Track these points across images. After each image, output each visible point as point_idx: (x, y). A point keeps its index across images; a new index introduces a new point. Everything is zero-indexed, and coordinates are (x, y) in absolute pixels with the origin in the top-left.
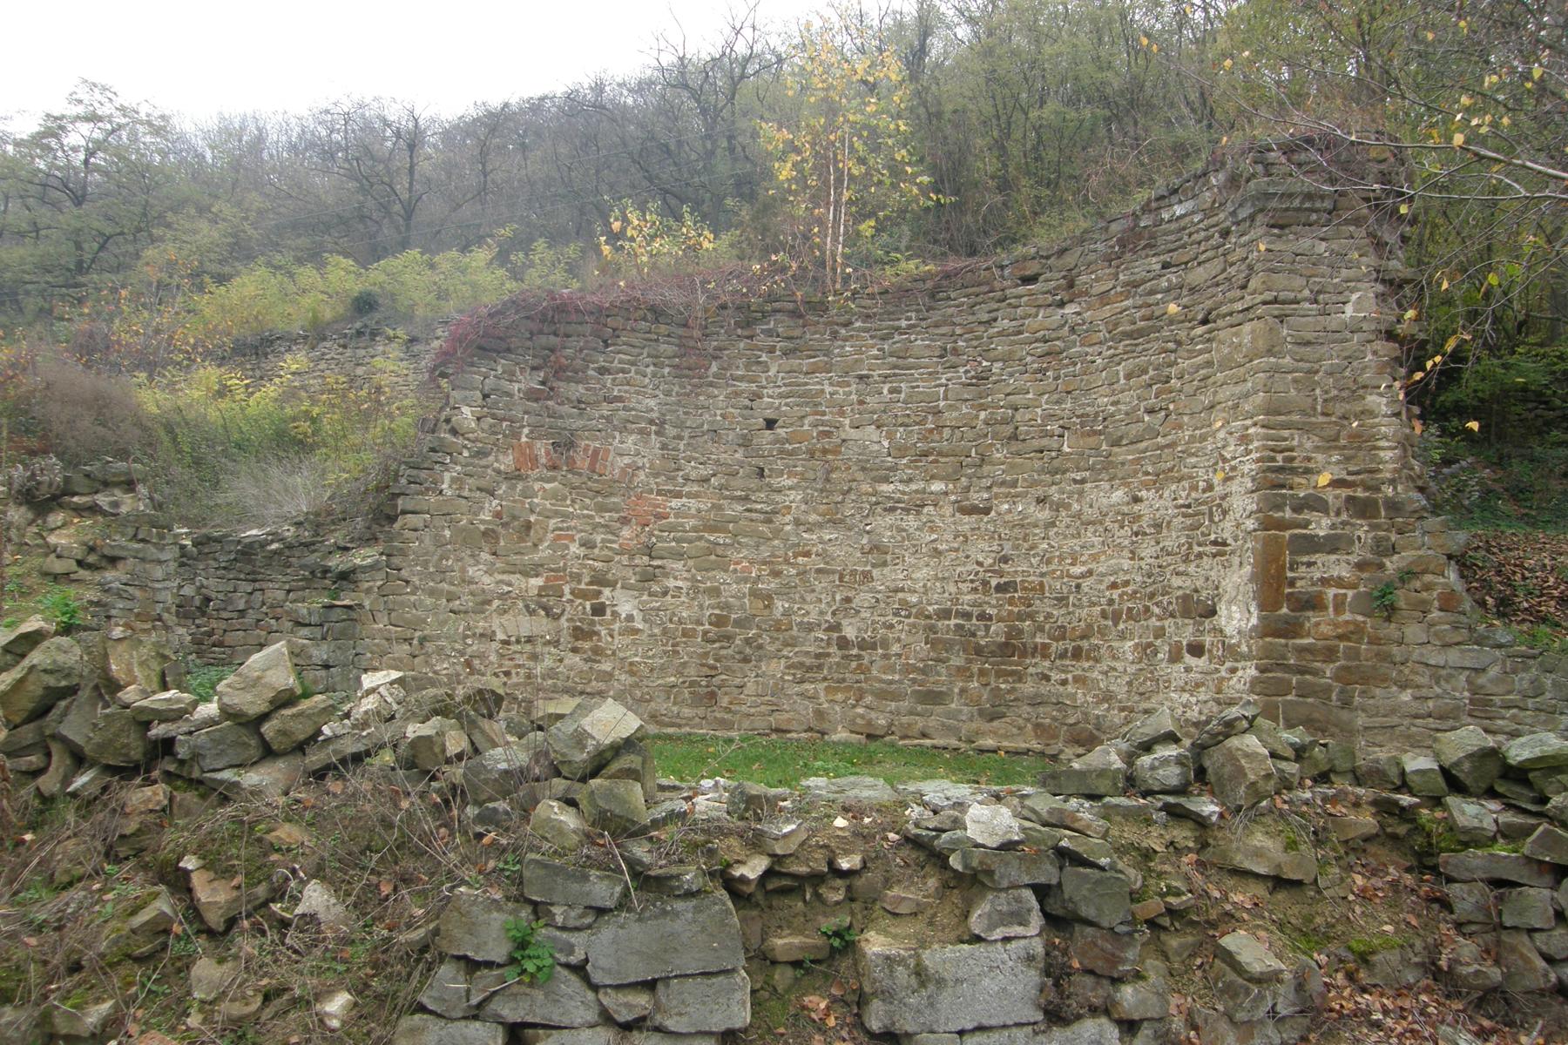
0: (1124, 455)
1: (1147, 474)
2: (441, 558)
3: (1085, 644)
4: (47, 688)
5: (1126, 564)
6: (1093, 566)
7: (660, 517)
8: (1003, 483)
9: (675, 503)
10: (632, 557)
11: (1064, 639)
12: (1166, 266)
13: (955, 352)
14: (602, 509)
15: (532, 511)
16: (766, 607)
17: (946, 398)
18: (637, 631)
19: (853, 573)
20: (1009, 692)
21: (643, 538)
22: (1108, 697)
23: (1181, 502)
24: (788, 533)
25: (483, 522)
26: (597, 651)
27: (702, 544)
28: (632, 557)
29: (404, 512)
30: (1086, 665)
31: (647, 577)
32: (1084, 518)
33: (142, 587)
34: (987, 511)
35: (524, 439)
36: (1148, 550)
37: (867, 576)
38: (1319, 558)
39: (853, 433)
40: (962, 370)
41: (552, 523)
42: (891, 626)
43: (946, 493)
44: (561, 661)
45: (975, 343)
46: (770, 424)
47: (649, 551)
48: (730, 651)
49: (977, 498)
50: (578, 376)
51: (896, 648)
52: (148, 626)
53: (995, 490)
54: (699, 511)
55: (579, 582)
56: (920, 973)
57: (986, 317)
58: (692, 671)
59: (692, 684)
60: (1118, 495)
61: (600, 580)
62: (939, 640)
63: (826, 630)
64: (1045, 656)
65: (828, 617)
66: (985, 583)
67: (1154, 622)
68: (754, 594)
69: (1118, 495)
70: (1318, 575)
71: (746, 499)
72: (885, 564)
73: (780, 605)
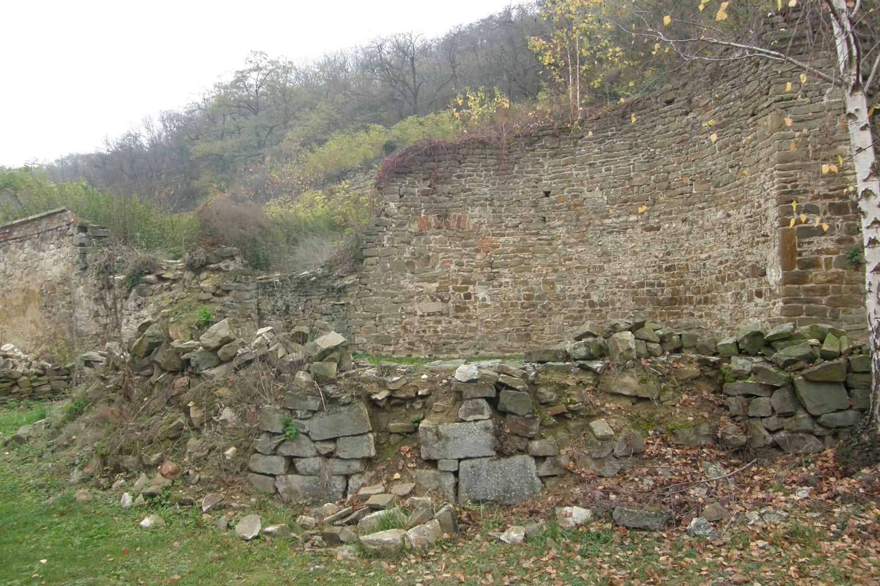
0: (721, 192)
1: (732, 201)
2: (386, 278)
3: (709, 295)
4: (150, 343)
5: (726, 251)
6: (711, 253)
7: (494, 247)
8: (665, 213)
9: (502, 239)
10: (482, 269)
11: (699, 293)
12: (733, 86)
13: (637, 146)
14: (465, 246)
15: (430, 251)
16: (552, 288)
17: (634, 171)
18: (488, 306)
19: (595, 267)
20: (675, 323)
21: (487, 259)
22: (721, 323)
24: (560, 249)
25: (405, 258)
26: (469, 317)
27: (517, 259)
28: (482, 269)
29: (366, 257)
30: (711, 306)
31: (491, 278)
32: (705, 228)
33: (240, 303)
34: (658, 229)
35: (423, 215)
36: (735, 243)
37: (602, 268)
38: (815, 239)
39: (589, 194)
40: (641, 155)
41: (441, 255)
42: (615, 293)
43: (637, 221)
44: (450, 323)
45: (646, 140)
46: (547, 194)
47: (491, 265)
48: (535, 312)
49: (653, 222)
50: (447, 181)
51: (618, 305)
52: (244, 320)
53: (662, 217)
54: (514, 242)
55: (457, 283)
56: (437, 434)
57: (649, 125)
58: (517, 324)
59: (518, 330)
60: (720, 214)
61: (467, 282)
62: (639, 299)
63: (583, 298)
64: (691, 303)
65: (584, 291)
66: (660, 267)
67: (740, 281)
68: (545, 282)
69: (720, 214)
70: (815, 248)
71: (538, 234)
72: (610, 261)
73: (559, 287)
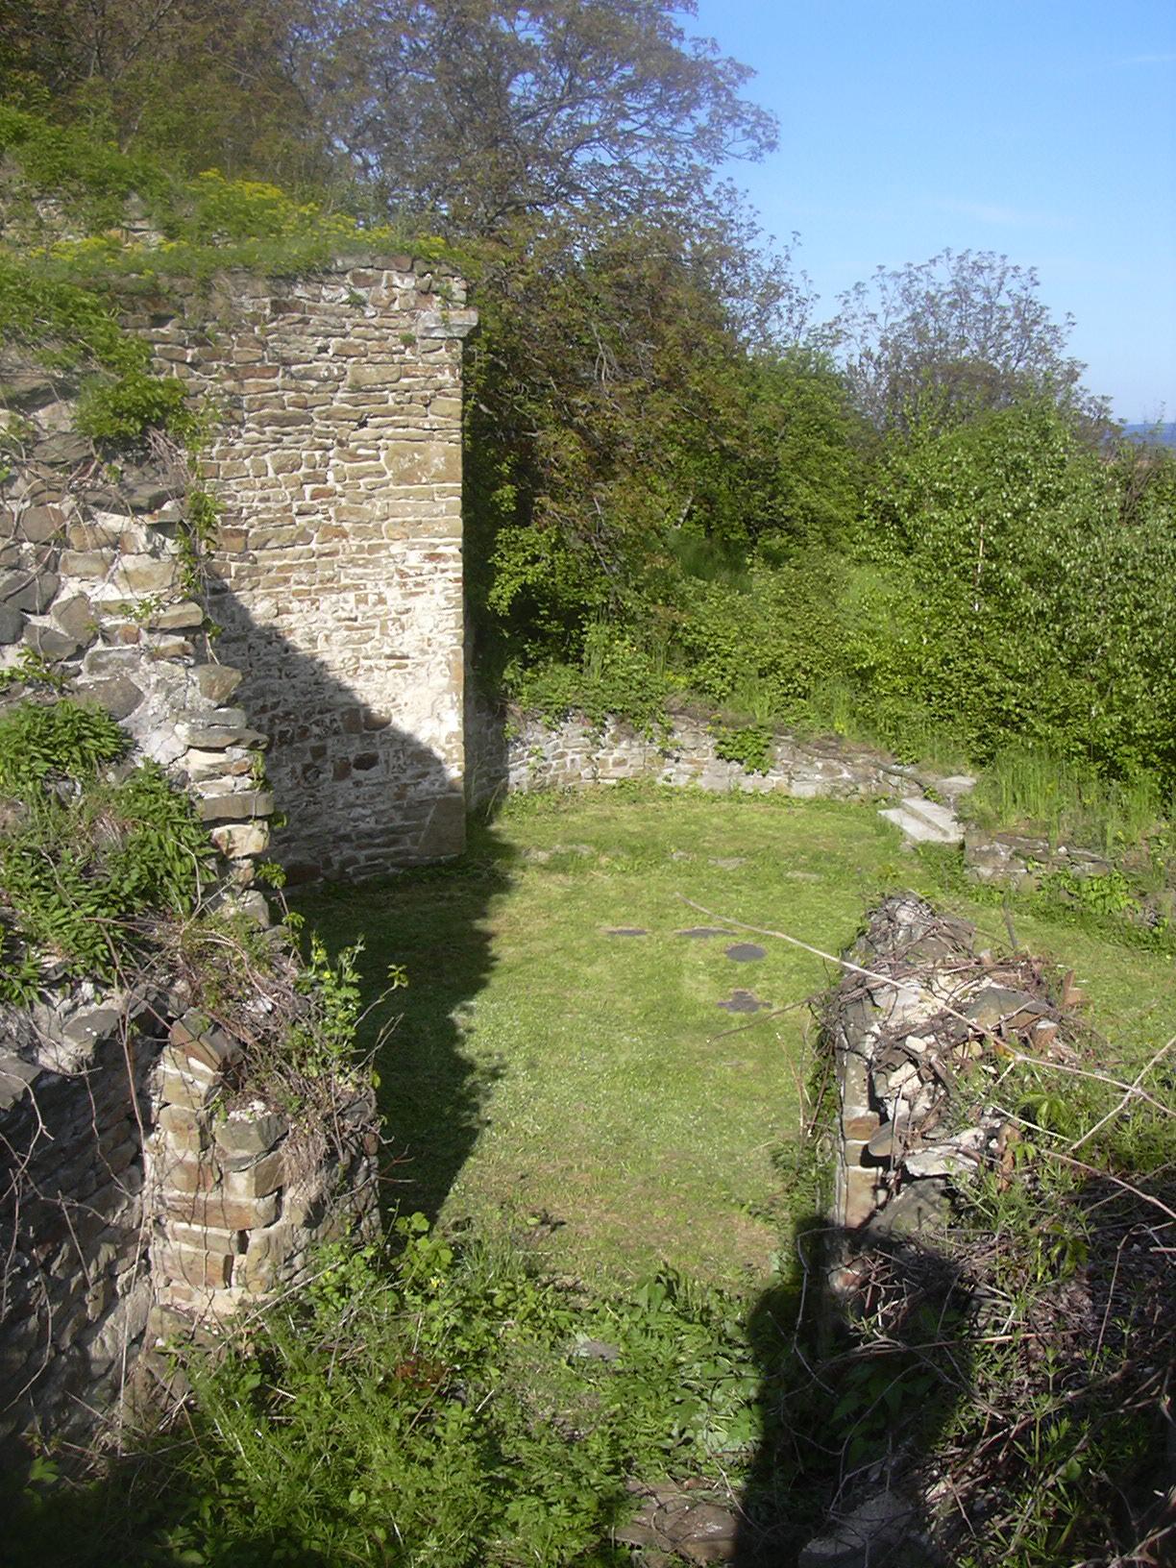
5: (276, 684)
23: (344, 615)
67: (313, 742)
